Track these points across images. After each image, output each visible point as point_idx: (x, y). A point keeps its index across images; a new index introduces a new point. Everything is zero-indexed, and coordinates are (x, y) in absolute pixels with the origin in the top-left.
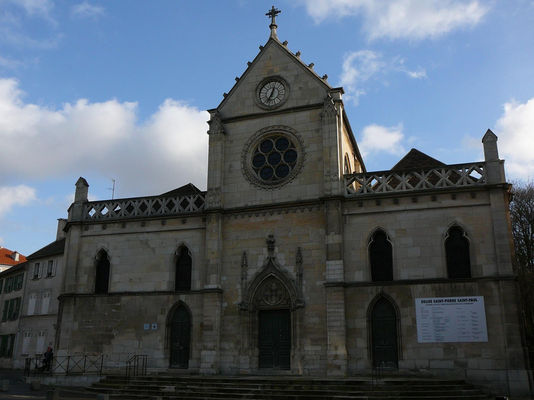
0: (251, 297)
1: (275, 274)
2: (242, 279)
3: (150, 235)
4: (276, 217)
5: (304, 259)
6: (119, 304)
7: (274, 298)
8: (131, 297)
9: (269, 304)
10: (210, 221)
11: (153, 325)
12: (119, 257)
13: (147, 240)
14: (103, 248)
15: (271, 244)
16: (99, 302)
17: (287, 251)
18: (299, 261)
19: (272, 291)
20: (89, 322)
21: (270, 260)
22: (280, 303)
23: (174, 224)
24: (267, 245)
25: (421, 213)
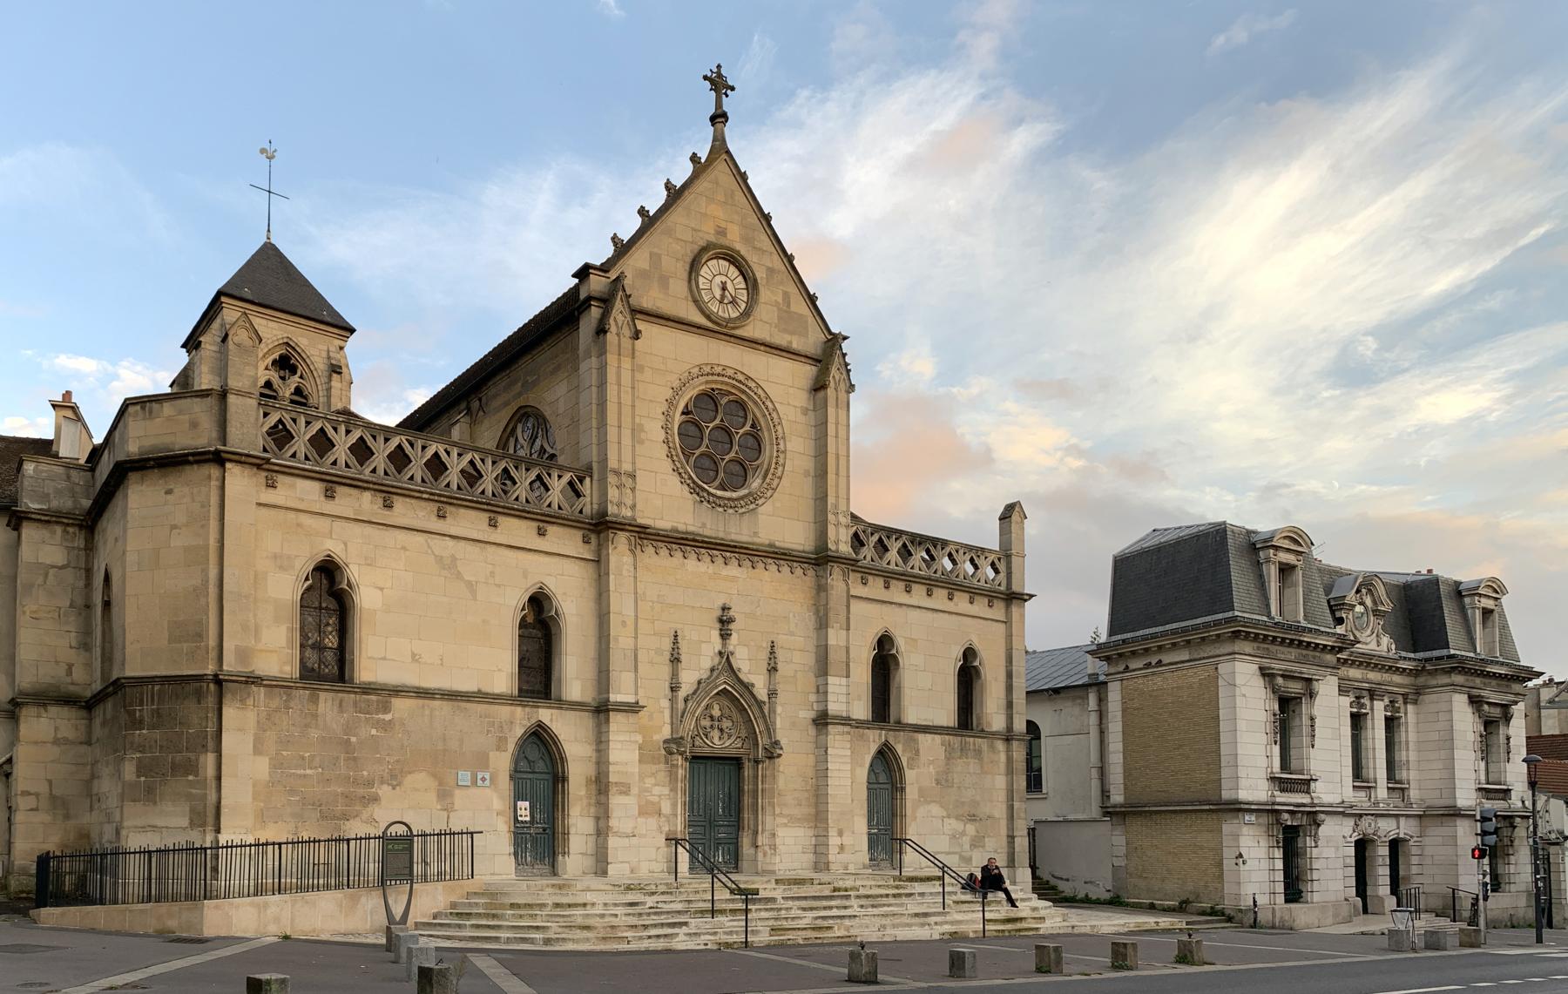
0: (689, 729)
1: (732, 687)
2: (674, 689)
3: (469, 547)
4: (733, 570)
5: (779, 666)
6: (388, 717)
7: (716, 734)
8: (421, 702)
9: (711, 744)
10: (615, 548)
11: (479, 777)
12: (381, 589)
13: (454, 558)
14: (332, 554)
15: (725, 623)
16: (327, 702)
17: (752, 643)
18: (772, 670)
19: (712, 717)
20: (303, 758)
21: (728, 658)
22: (731, 745)
23: (516, 530)
24: (718, 626)
25: (936, 615)
